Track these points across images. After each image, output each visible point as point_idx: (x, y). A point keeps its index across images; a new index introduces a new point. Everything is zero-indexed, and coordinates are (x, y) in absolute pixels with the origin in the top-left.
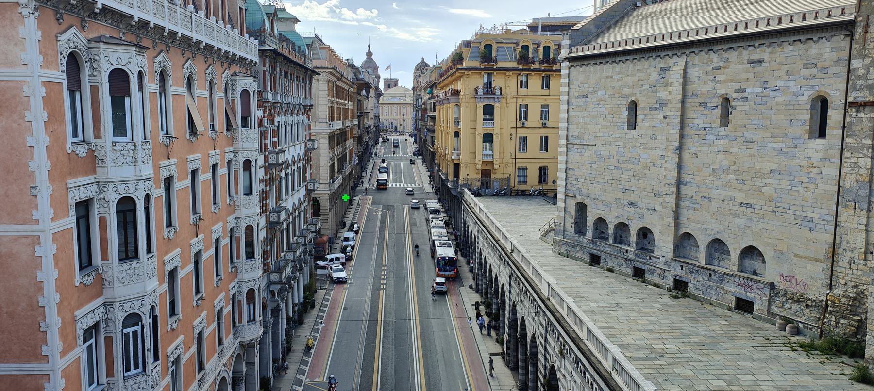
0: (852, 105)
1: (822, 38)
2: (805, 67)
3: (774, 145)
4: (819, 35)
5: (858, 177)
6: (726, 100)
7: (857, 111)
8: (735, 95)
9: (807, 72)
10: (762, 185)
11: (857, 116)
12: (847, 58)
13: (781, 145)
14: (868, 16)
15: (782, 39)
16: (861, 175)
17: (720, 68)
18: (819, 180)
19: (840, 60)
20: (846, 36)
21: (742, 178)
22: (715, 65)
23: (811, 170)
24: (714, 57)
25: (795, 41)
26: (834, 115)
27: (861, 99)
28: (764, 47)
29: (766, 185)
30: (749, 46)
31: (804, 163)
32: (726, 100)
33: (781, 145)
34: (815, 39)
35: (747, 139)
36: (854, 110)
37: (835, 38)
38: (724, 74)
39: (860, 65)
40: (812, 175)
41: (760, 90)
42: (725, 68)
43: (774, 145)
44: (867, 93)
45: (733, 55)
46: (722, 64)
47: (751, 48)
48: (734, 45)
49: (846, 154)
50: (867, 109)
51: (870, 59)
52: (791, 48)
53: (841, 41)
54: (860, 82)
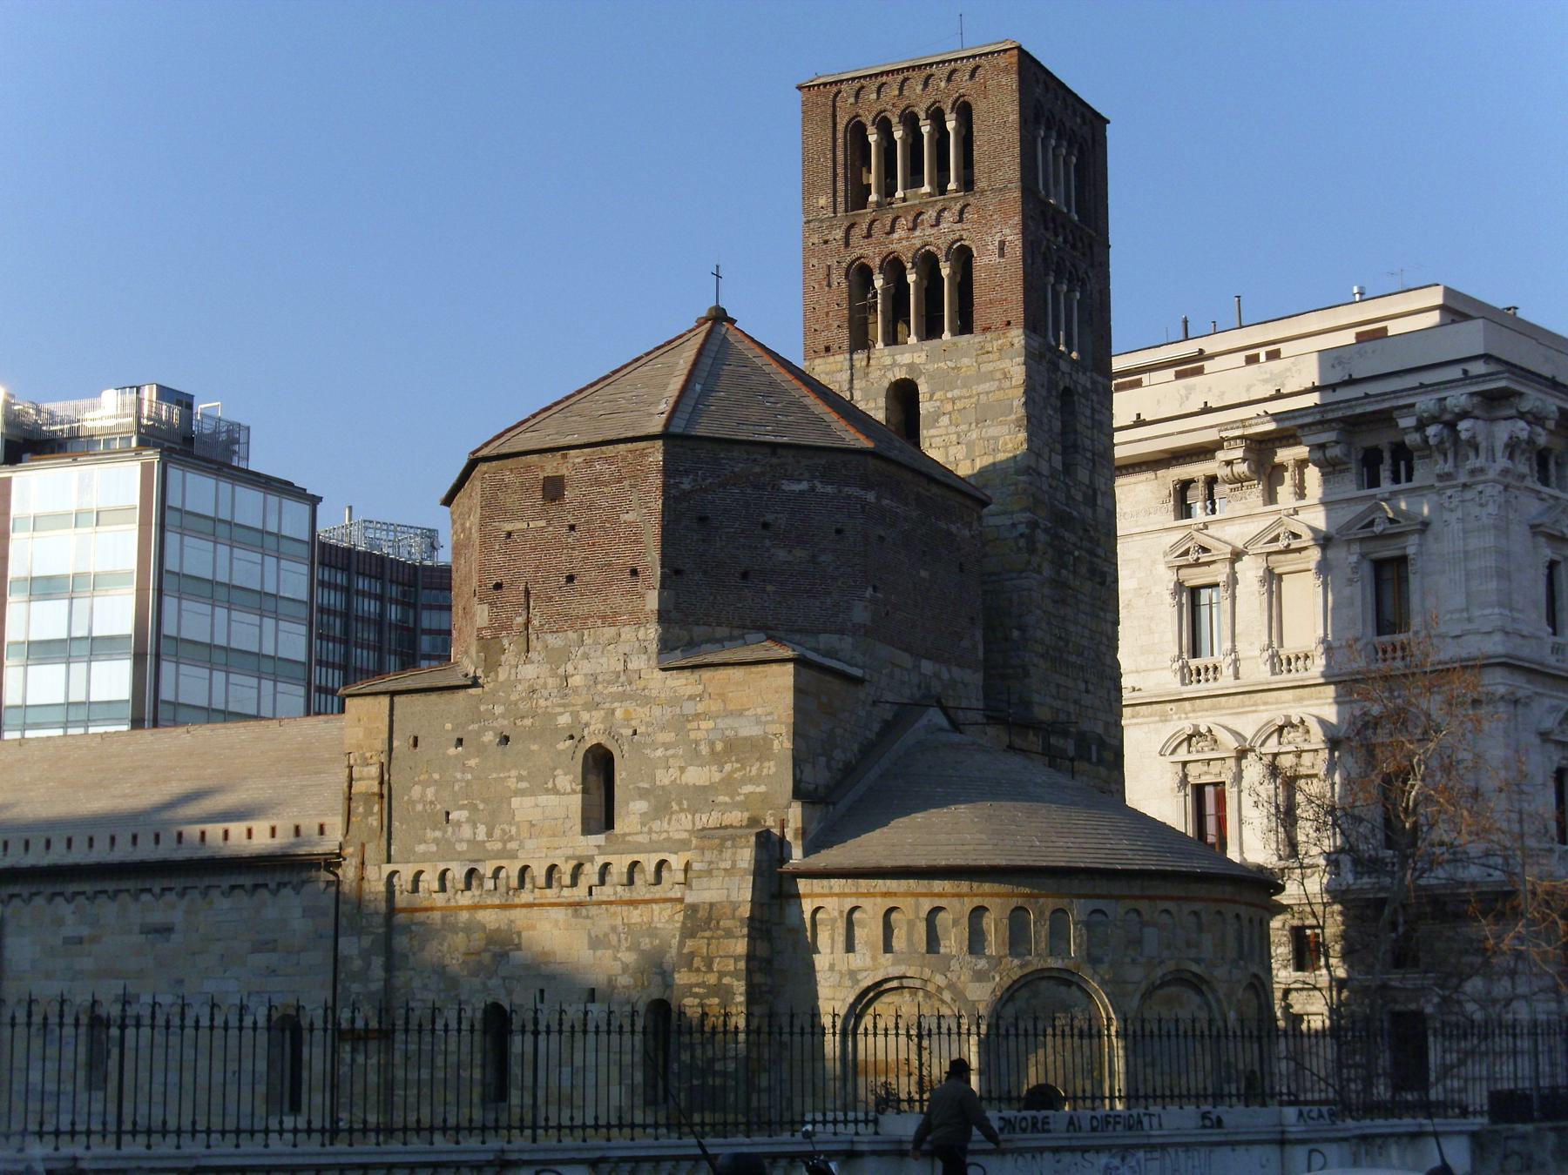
1: (285, 885)
6: (98, 1023)
9: (260, 960)
12: (332, 933)
14: (363, 845)
15: (207, 881)
17: (80, 941)
19: (321, 937)
22: (68, 931)
24: (64, 909)
25: (233, 888)
26: (315, 1056)
28: (171, 897)
34: (272, 886)
39: (354, 951)
42: (95, 939)
45: (108, 910)
46: (85, 931)
47: (145, 897)
51: (371, 938)
52: (225, 903)
54: (356, 987)
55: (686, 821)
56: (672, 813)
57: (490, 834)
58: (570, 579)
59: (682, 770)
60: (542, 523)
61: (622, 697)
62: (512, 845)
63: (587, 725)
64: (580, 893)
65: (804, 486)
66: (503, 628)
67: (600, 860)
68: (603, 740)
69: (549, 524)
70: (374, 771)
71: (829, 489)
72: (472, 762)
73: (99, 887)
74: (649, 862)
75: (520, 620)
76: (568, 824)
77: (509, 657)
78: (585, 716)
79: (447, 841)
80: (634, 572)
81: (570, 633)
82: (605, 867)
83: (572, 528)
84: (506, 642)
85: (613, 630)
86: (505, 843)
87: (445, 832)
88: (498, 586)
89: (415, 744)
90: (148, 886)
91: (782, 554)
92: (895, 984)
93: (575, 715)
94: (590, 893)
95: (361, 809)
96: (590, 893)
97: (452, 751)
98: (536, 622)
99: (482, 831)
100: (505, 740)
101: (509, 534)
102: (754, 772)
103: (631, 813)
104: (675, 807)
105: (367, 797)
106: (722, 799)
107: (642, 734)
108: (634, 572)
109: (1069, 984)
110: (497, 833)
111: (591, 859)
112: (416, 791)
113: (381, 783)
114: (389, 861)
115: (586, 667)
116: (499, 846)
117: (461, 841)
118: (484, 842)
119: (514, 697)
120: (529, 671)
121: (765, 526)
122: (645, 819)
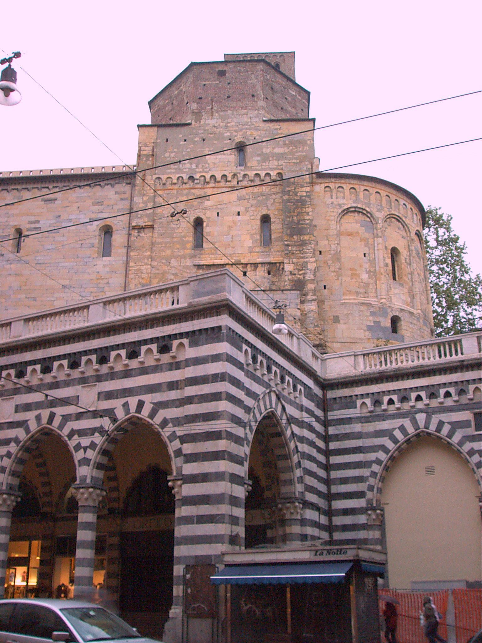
0: (134, 228)
1: (108, 184)
2: (94, 204)
3: (66, 264)
4: (105, 182)
5: (141, 280)
6: (19, 232)
7: (139, 232)
8: (28, 226)
10: (53, 299)
11: (139, 235)
13: (72, 264)
16: (143, 278)
18: (106, 289)
20: (127, 184)
21: (33, 295)
23: (99, 281)
26: (119, 238)
27: (142, 224)
29: (57, 299)
30: (44, 188)
31: (93, 277)
32: (19, 232)
33: (72, 264)
35: (40, 262)
36: (136, 231)
37: (117, 186)
38: (17, 209)
39: (141, 201)
40: (100, 286)
41: (54, 221)
43: (66, 264)
44: (146, 220)
48: (30, 186)
49: (131, 264)
50: (146, 230)
53: (122, 187)
55: (276, 163)
56: (270, 161)
57: (197, 167)
58: (229, 97)
59: (273, 149)
60: (218, 82)
61: (250, 129)
62: (205, 170)
63: (236, 136)
64: (234, 183)
65: (294, 93)
66: (202, 109)
67: (243, 173)
68: (242, 140)
69: (220, 82)
70: (151, 148)
71: (299, 98)
72: (190, 146)
73: (24, 187)
74: (263, 174)
75: (210, 107)
76: (229, 164)
77: (205, 116)
78: (235, 134)
79: (180, 169)
80: (253, 96)
81: (229, 111)
82: (245, 175)
83: (229, 84)
84: (203, 113)
85: (245, 111)
86: (203, 169)
87: (179, 166)
88: (200, 98)
89: (167, 140)
90: (47, 186)
91: (290, 109)
92: (353, 209)
93: (231, 133)
94: (238, 183)
95: (145, 159)
96: (238, 183)
97: (182, 143)
98: (215, 108)
99: (194, 166)
100: (204, 140)
101: (205, 85)
102: (300, 149)
103: (253, 161)
104: (271, 159)
105: (147, 156)
106: (289, 156)
107: (258, 139)
108: (253, 96)
109: (399, 221)
110: (200, 166)
111: (239, 173)
112: (167, 155)
113: (153, 151)
114: (155, 174)
115: (235, 120)
116: (201, 170)
117: (186, 168)
118: (195, 169)
119: (207, 128)
120: (212, 122)
121: (286, 99)
122: (259, 162)
